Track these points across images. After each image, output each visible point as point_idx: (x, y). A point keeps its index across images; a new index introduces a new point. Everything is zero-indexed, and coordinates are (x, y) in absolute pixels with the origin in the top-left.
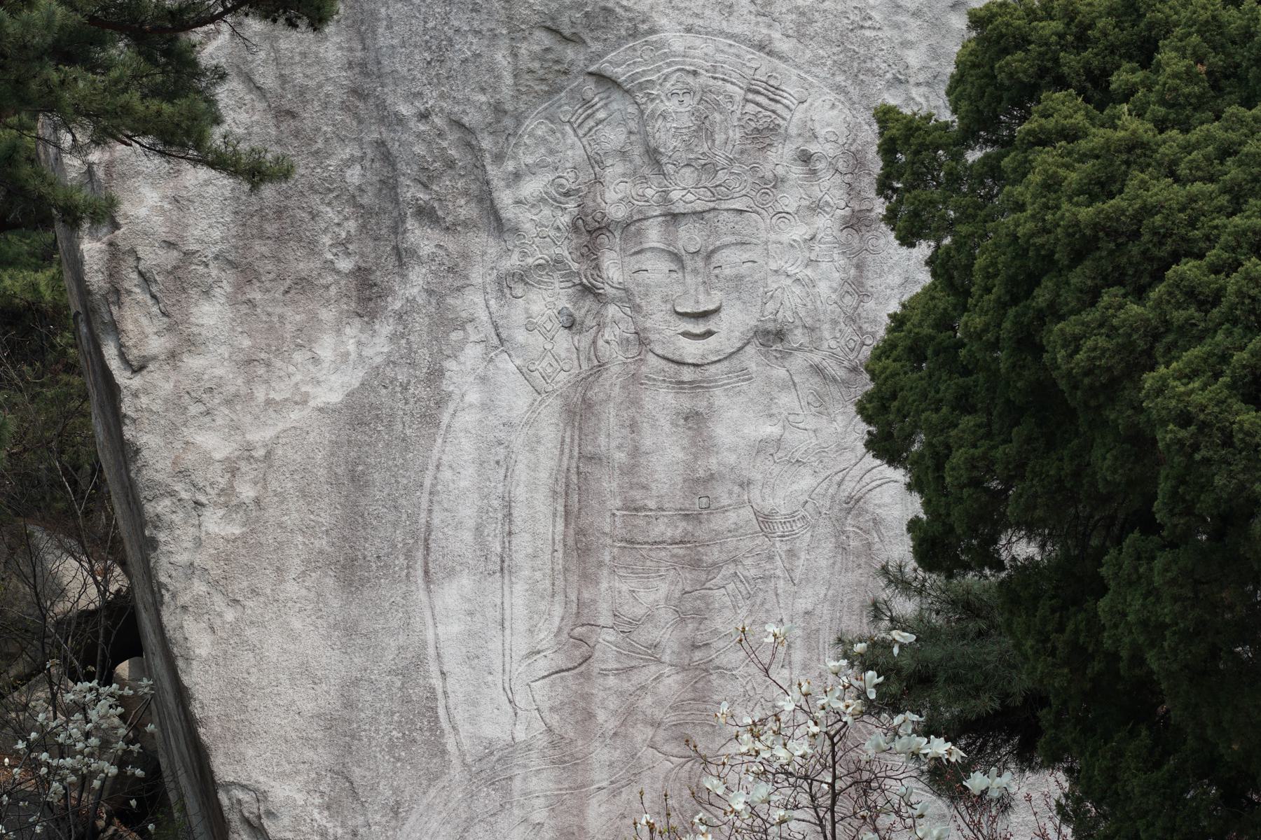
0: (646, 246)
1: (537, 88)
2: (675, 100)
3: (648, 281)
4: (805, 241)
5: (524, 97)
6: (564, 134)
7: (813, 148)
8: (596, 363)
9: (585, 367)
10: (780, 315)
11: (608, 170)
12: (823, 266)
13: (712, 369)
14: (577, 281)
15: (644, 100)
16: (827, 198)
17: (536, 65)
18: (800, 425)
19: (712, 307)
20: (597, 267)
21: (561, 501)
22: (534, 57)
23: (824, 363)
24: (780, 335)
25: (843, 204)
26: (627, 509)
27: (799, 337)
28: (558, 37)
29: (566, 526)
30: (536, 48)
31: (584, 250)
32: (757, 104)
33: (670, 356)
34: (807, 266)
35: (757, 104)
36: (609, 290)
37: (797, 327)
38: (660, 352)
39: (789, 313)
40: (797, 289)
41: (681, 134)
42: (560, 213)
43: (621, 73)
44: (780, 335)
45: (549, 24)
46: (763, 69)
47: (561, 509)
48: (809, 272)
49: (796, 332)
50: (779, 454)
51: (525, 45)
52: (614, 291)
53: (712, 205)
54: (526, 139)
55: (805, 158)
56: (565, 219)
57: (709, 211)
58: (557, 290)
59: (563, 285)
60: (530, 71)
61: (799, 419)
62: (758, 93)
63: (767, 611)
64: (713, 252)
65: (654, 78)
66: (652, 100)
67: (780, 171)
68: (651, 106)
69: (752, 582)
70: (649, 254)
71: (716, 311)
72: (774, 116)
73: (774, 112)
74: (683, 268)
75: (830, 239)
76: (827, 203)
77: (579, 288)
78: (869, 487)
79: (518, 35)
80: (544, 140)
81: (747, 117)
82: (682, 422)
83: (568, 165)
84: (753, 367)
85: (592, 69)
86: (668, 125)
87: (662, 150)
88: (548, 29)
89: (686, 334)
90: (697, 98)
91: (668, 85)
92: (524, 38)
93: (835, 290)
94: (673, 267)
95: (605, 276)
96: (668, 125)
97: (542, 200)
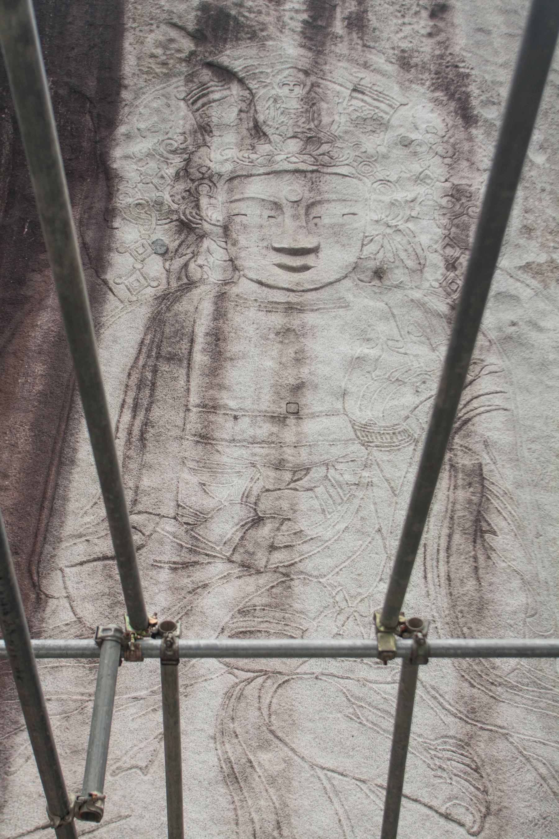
0: (246, 196)
1: (157, 70)
2: (286, 89)
3: (245, 222)
4: (406, 201)
5: (145, 76)
6: (178, 108)
7: (413, 136)
8: (185, 281)
9: (174, 284)
10: (380, 255)
11: (215, 139)
12: (424, 223)
13: (310, 296)
14: (175, 217)
15: (256, 86)
16: (427, 172)
17: (159, 51)
18: (400, 350)
19: (310, 246)
20: (197, 206)
21: (131, 394)
22: (159, 44)
23: (426, 299)
24: (379, 274)
25: (443, 180)
26: (205, 406)
27: (398, 275)
28: (183, 33)
29: (134, 417)
30: (161, 38)
31: (186, 194)
32: (363, 100)
33: (264, 280)
34: (407, 221)
35: (363, 100)
36: (206, 226)
37: (397, 267)
38: (254, 277)
39: (390, 255)
40: (398, 238)
41: (289, 113)
42: (165, 167)
43: (237, 66)
44: (379, 274)
45: (176, 20)
46: (368, 79)
47: (130, 401)
48: (410, 225)
49: (396, 271)
50: (377, 372)
51: (152, 35)
52: (212, 227)
53: (315, 168)
54: (141, 109)
55: (406, 143)
56: (171, 171)
57: (312, 172)
58: (153, 226)
59: (160, 222)
60: (152, 56)
61: (400, 345)
62: (363, 93)
63: (362, 519)
64: (313, 204)
65: (269, 71)
66: (266, 86)
67: (383, 150)
68: (262, 92)
69: (345, 487)
70: (249, 203)
71: (315, 250)
72: (377, 111)
73: (378, 108)
74: (283, 213)
75: (431, 203)
76: (427, 177)
77: (178, 223)
78: (477, 411)
79: (147, 28)
80: (157, 111)
81: (352, 108)
82: (272, 336)
83: (178, 131)
84: (350, 297)
85: (210, 59)
86: (278, 106)
87: (270, 123)
88: (175, 25)
89: (281, 266)
90: (307, 88)
91: (280, 77)
92: (151, 31)
93: (437, 242)
94: (273, 213)
95: (203, 214)
96: (278, 106)
97: (149, 155)
